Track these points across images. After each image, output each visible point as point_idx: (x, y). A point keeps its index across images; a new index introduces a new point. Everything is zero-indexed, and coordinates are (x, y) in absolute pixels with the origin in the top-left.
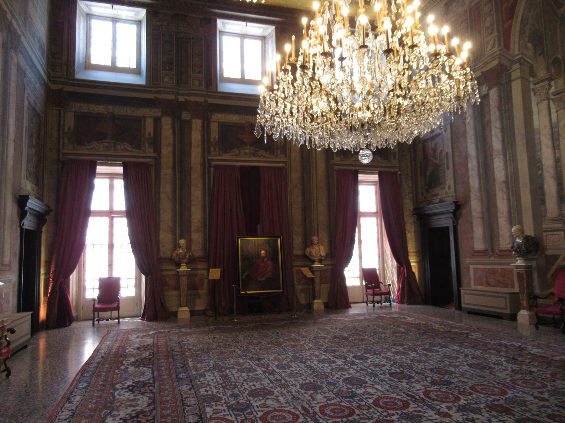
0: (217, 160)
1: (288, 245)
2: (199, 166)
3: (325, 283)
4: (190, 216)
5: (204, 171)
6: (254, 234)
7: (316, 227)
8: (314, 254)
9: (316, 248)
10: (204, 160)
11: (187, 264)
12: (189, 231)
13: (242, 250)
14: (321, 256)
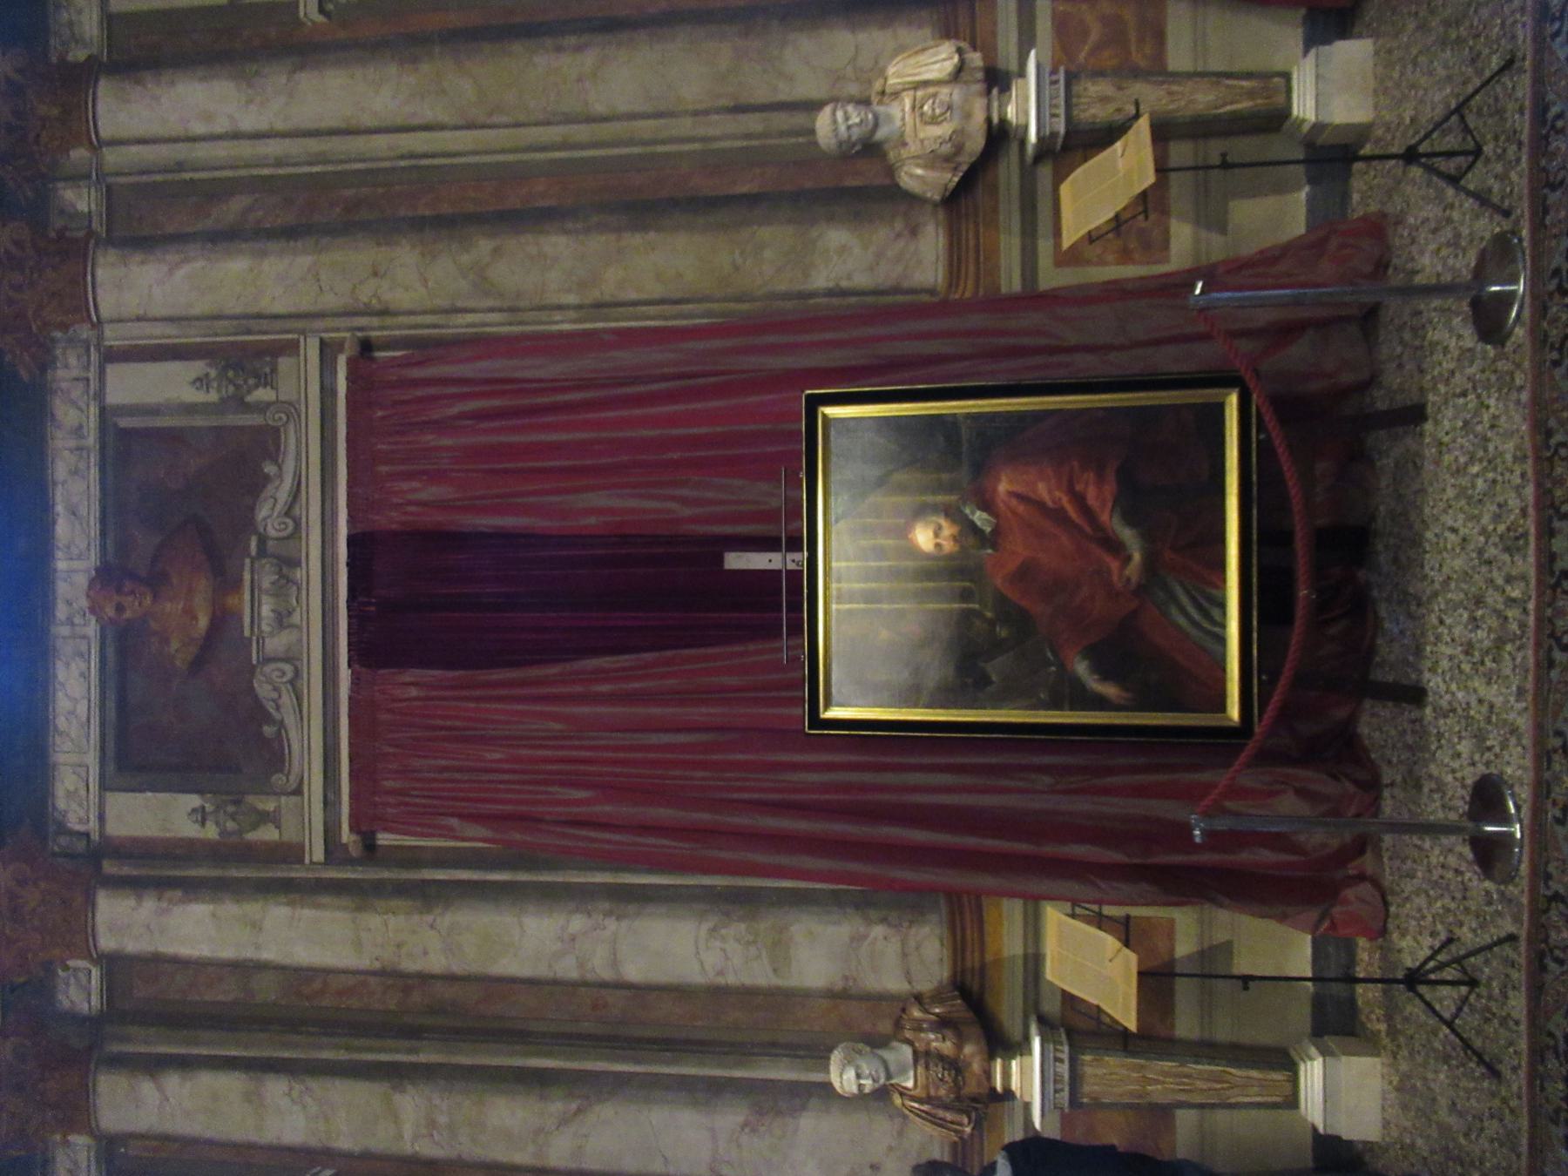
0: (329, 804)
1: (877, 346)
2: (373, 920)
3: (1160, 36)
4: (680, 992)
5: (402, 890)
6: (785, 605)
7: (754, 123)
8: (944, 130)
9: (899, 113)
10: (338, 888)
11: (1002, 1045)
12: (781, 1000)
13: (910, 697)
14: (958, 74)
